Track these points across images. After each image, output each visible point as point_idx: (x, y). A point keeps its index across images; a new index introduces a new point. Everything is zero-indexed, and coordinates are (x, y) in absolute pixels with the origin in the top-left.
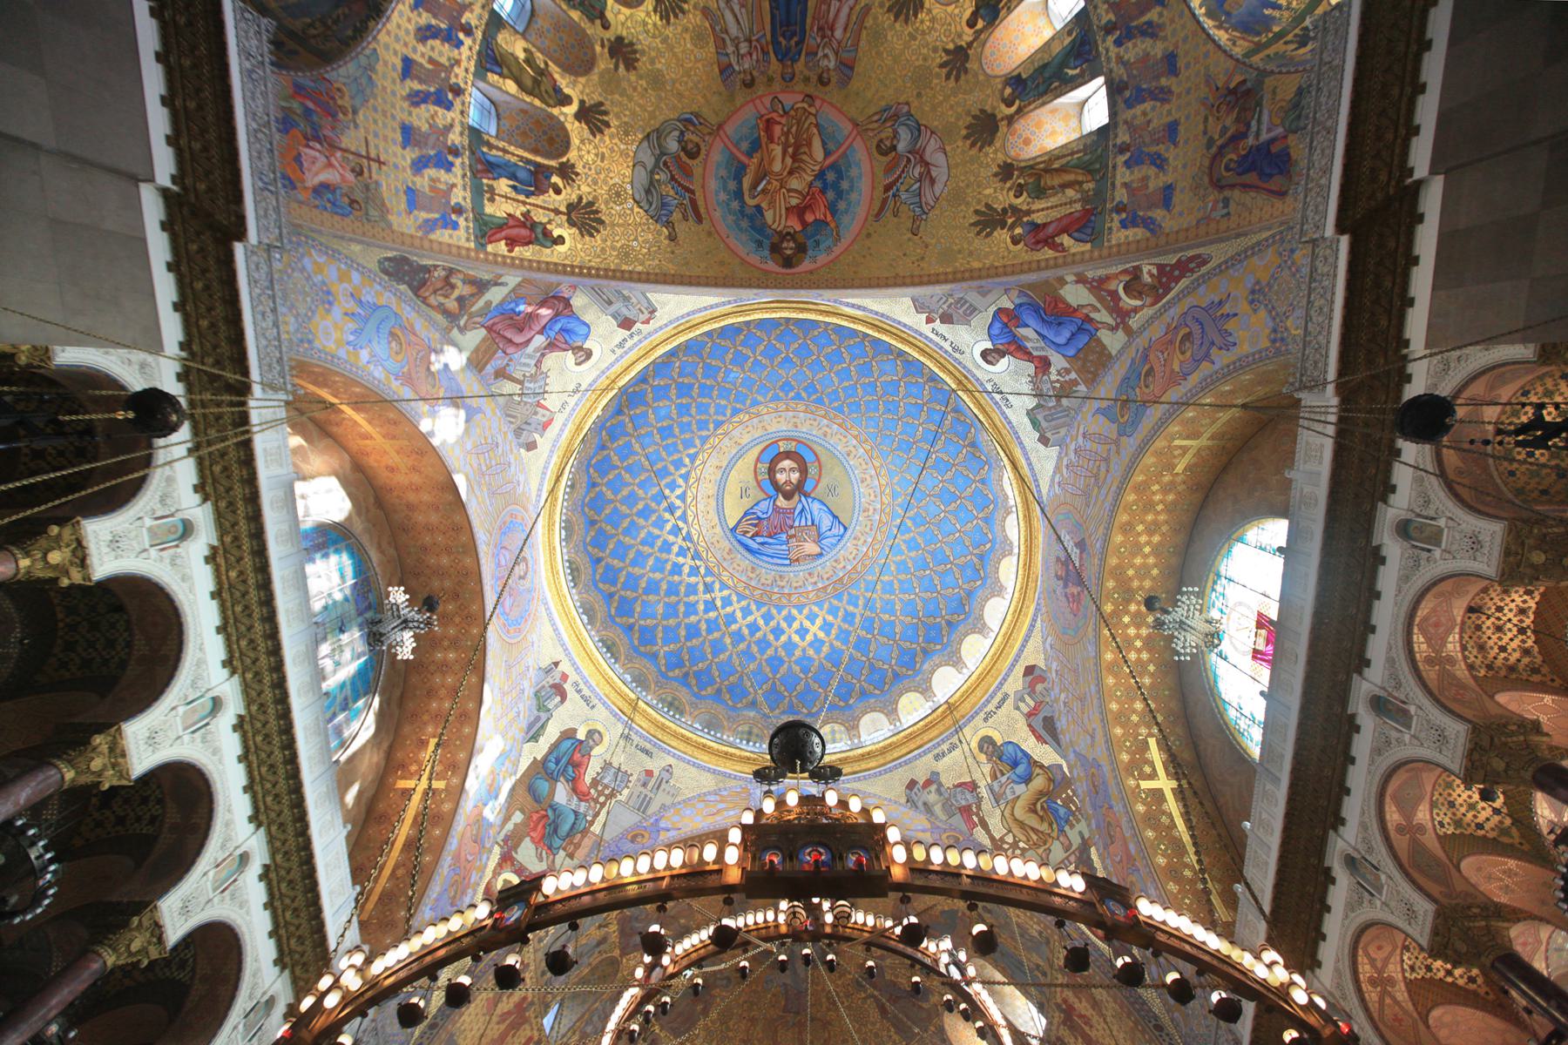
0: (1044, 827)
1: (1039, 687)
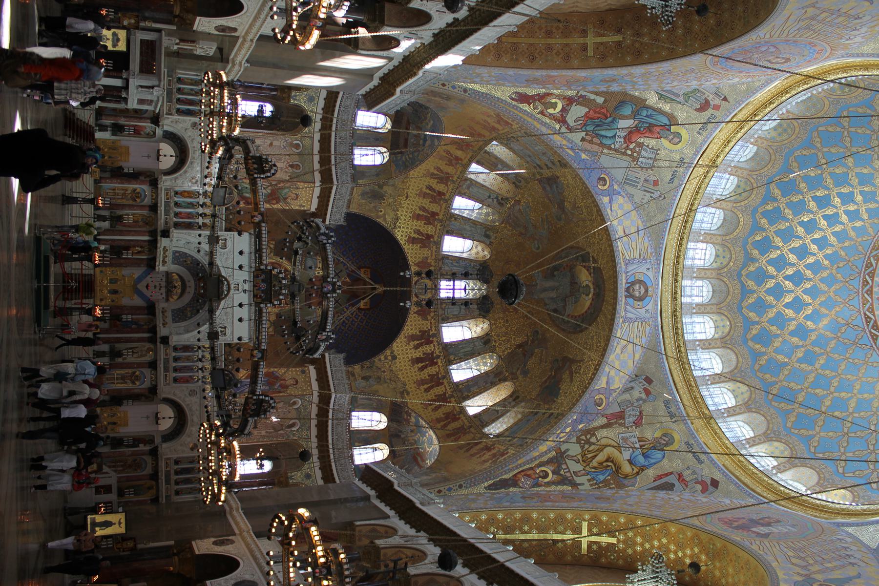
0: (595, 463)
1: (699, 487)
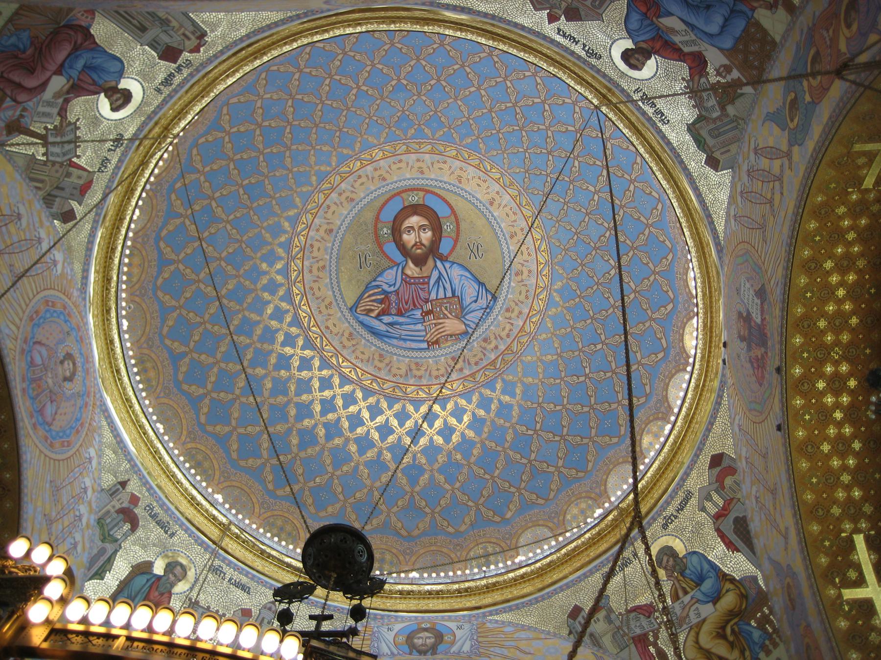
1: (728, 481)
